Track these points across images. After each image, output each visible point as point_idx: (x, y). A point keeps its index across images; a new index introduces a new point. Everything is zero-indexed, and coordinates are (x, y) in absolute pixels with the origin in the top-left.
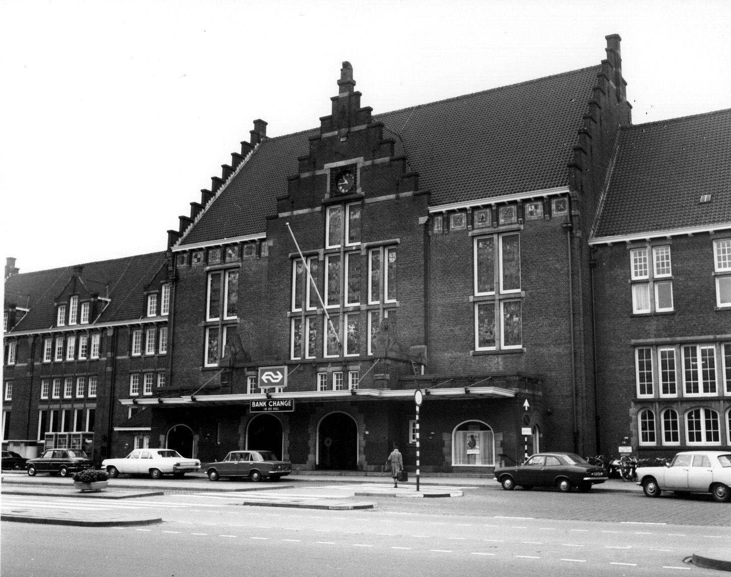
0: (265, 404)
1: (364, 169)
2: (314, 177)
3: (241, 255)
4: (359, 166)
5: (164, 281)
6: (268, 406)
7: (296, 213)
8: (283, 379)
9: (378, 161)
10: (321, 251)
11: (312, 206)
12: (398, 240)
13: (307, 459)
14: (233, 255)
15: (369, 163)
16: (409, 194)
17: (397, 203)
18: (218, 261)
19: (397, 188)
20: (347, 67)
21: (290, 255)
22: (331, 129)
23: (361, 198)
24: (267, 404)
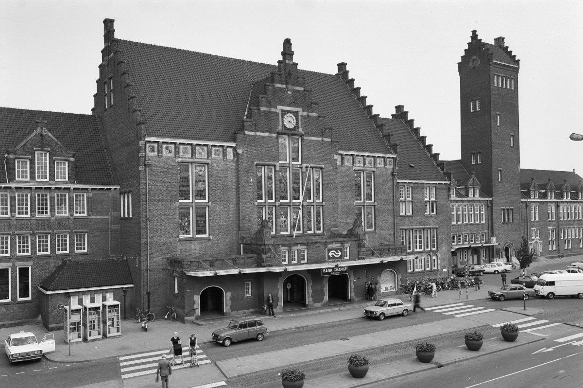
0: (331, 270)
1: (302, 116)
2: (270, 112)
3: (209, 154)
4: (300, 114)
5: (40, 149)
6: (333, 272)
7: (258, 134)
8: (328, 253)
9: (311, 114)
10: (277, 164)
11: (270, 132)
12: (323, 166)
13: (323, 299)
14: (203, 154)
15: (305, 114)
16: (329, 140)
17: (322, 144)
18: (189, 155)
19: (322, 134)
20: (287, 43)
21: (256, 163)
22: (281, 82)
23: (301, 135)
24: (333, 270)
